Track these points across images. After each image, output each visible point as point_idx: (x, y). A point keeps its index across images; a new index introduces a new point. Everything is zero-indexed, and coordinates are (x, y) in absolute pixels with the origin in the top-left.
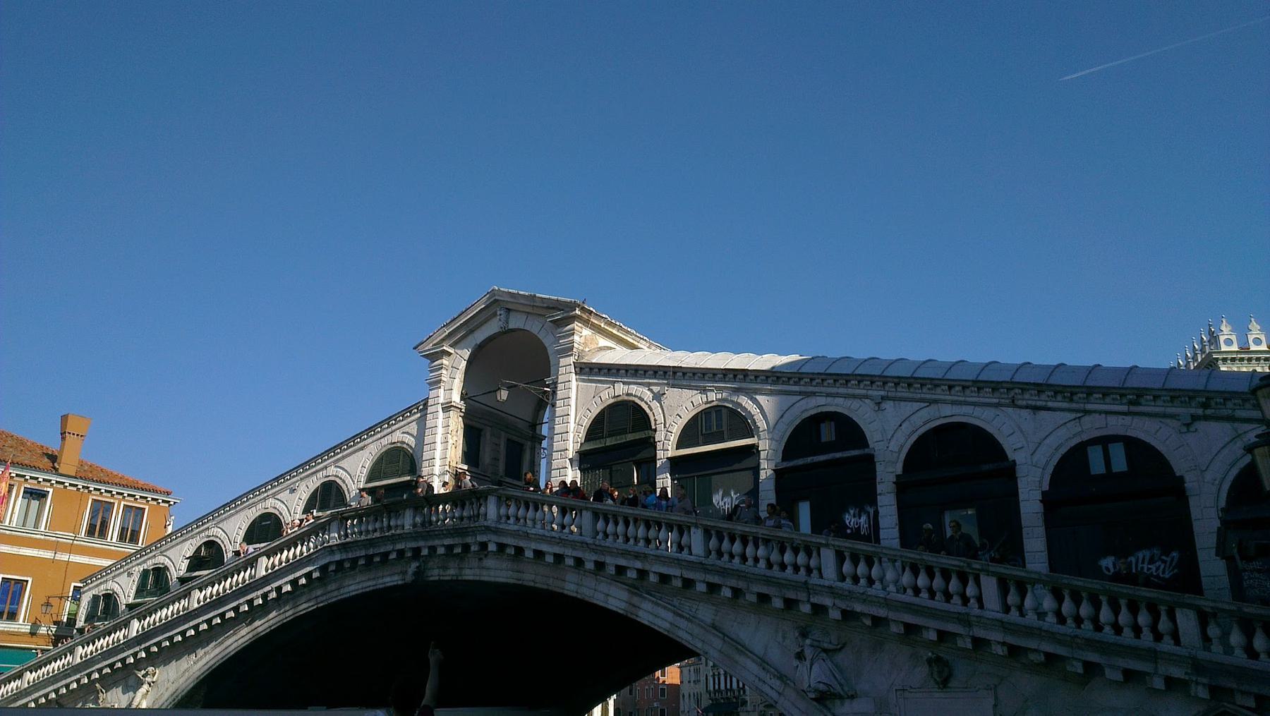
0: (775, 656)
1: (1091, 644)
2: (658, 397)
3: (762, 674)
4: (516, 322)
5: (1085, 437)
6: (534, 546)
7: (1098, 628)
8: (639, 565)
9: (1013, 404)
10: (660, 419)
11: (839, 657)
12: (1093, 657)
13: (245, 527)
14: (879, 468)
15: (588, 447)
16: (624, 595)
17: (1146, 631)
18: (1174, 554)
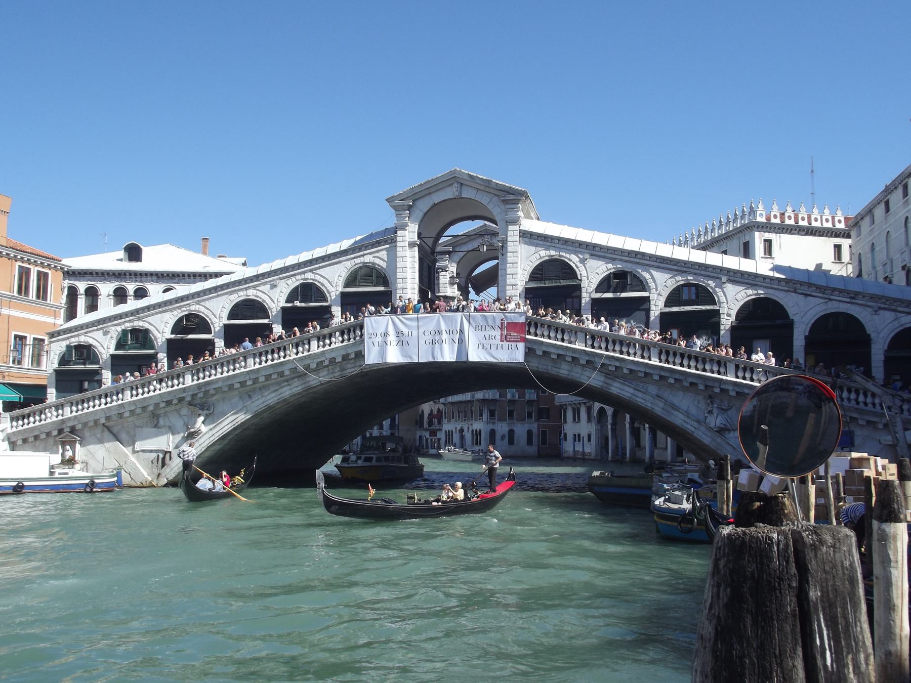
0: (693, 411)
1: (857, 410)
2: (583, 261)
3: (686, 419)
4: (467, 193)
5: (829, 312)
6: (544, 349)
7: (858, 403)
8: (617, 364)
9: (795, 292)
10: (584, 273)
11: (729, 412)
12: (855, 415)
13: (229, 307)
14: (722, 316)
15: (532, 285)
16: (602, 379)
17: (878, 406)
18: (862, 368)
